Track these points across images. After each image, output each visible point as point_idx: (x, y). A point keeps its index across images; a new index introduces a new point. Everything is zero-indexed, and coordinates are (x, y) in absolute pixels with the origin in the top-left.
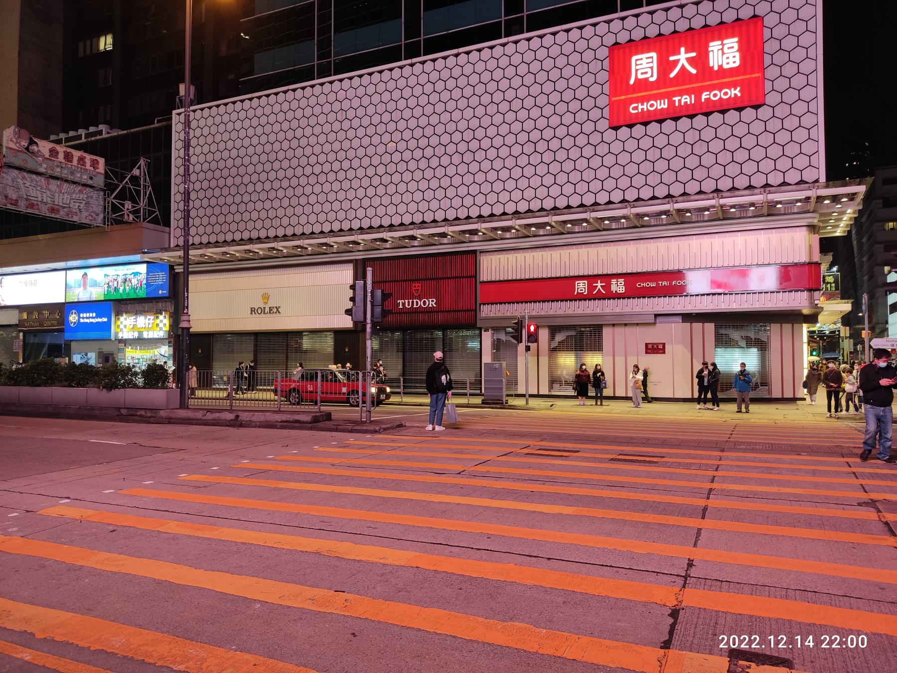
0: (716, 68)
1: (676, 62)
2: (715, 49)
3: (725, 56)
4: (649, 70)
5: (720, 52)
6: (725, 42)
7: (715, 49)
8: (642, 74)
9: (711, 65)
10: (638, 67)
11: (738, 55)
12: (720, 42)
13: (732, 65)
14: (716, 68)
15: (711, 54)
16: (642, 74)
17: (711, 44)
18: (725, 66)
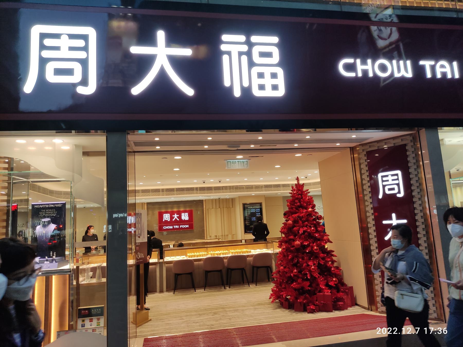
0: (237, 93)
1: (145, 62)
2: (235, 50)
3: (255, 70)
4: (78, 68)
5: (244, 58)
6: (254, 39)
7: (235, 50)
8: (58, 72)
9: (227, 83)
10: (46, 54)
11: (280, 72)
12: (242, 38)
13: (268, 93)
14: (237, 93)
15: (225, 58)
16: (58, 72)
17: (225, 37)
18: (257, 93)
